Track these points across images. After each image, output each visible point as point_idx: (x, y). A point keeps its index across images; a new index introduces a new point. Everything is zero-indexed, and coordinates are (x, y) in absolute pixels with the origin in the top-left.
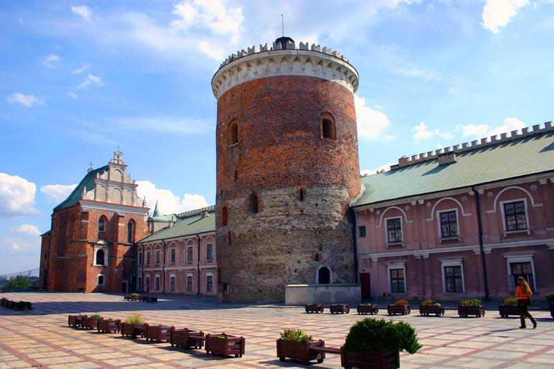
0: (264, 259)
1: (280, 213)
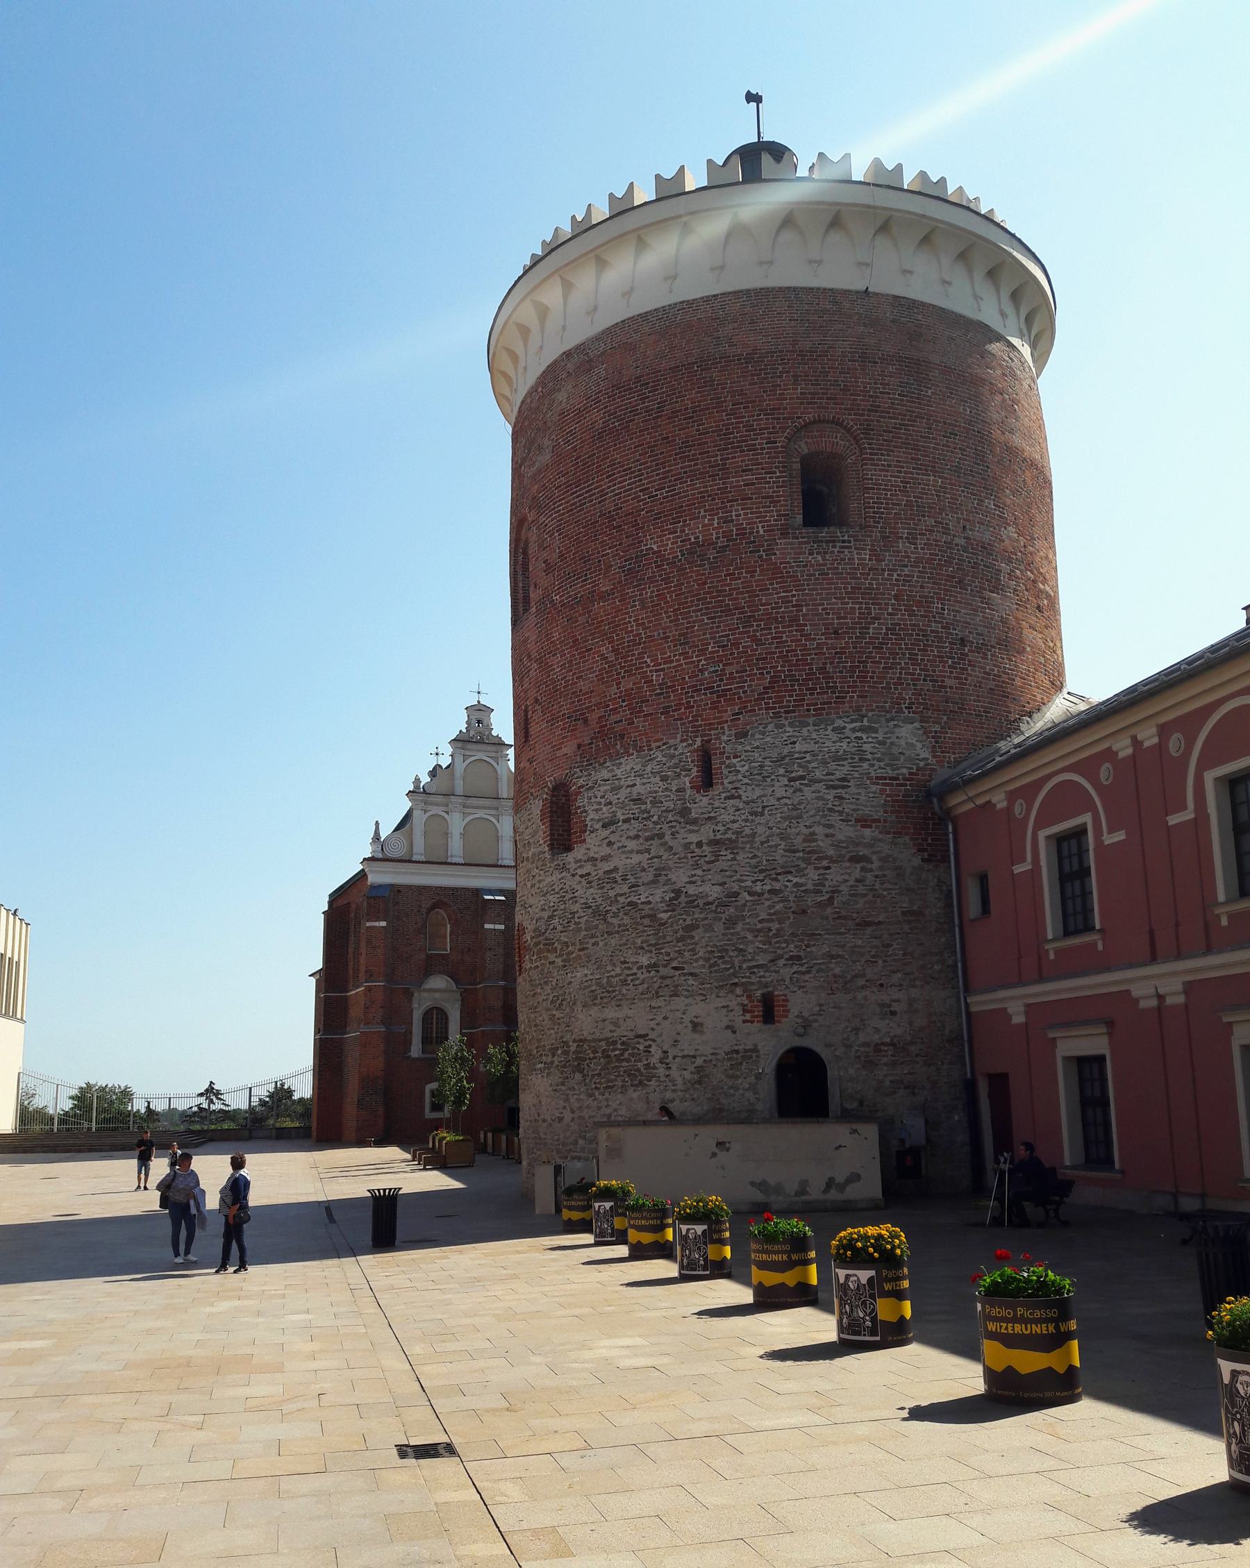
0: (586, 1022)
1: (632, 845)
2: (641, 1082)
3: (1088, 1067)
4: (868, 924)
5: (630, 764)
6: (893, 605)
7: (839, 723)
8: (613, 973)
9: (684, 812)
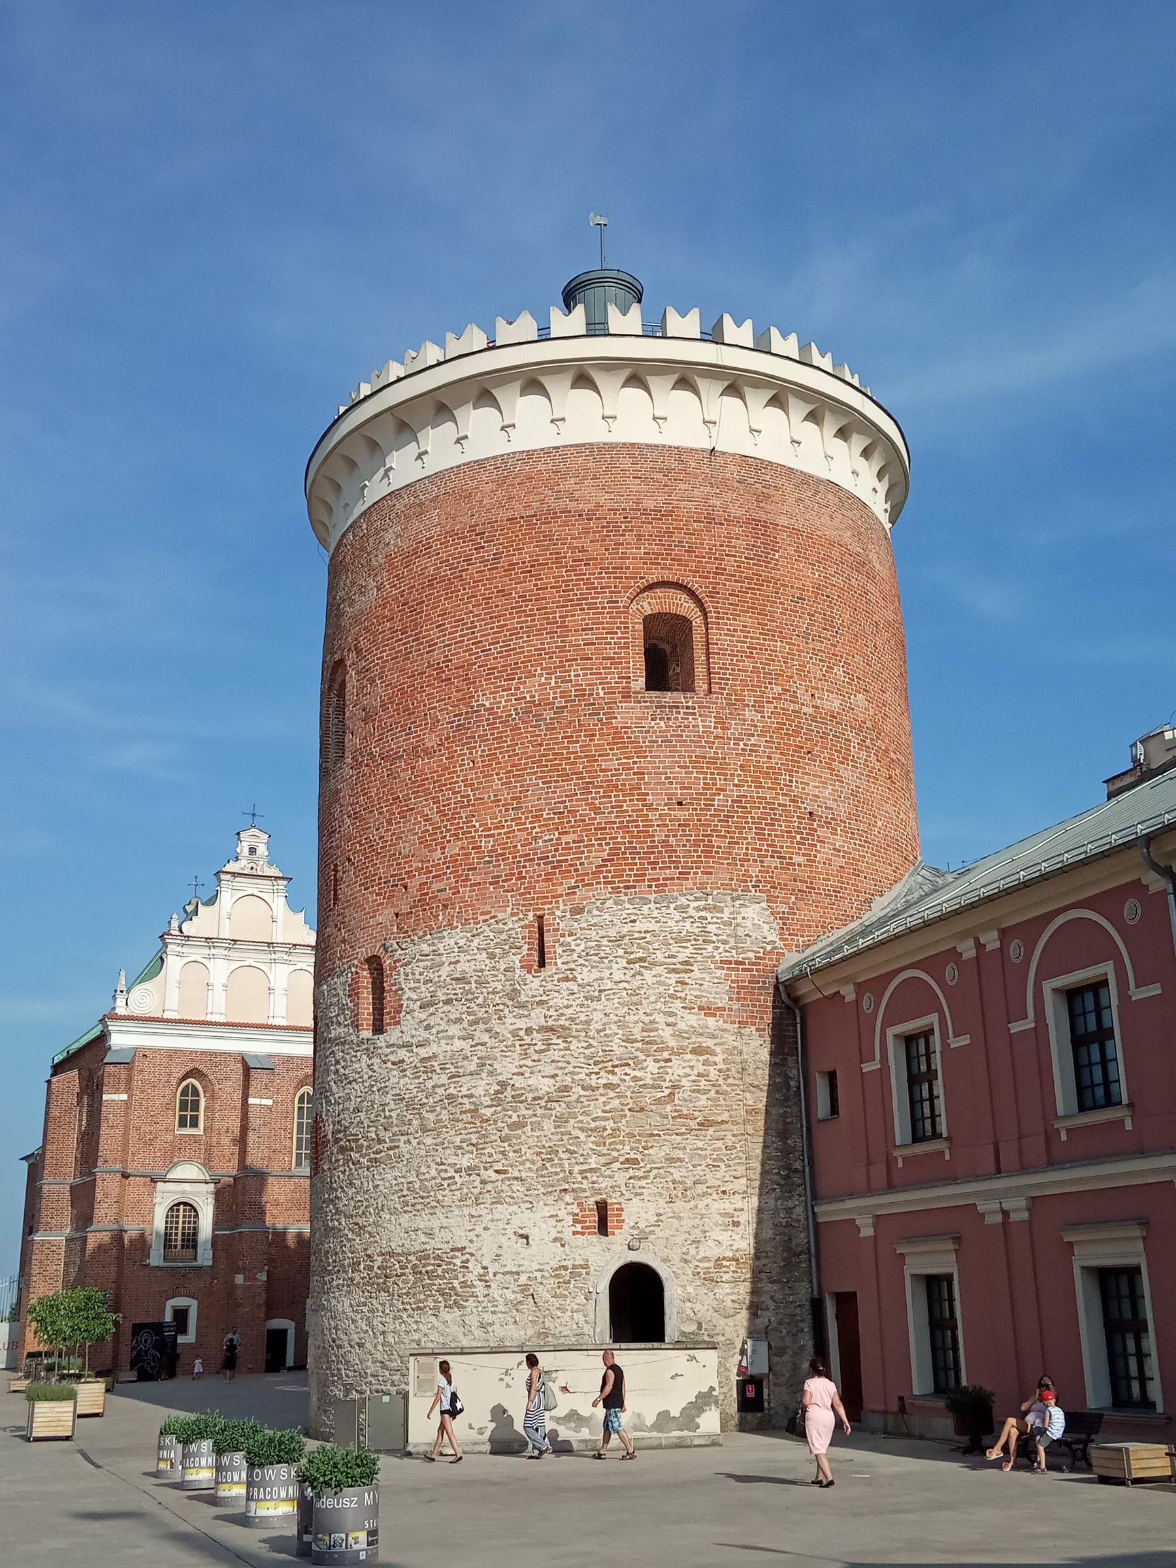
1: (454, 1030)
2: (455, 1302)
3: (935, 1287)
4: (711, 1123)
5: (452, 939)
6: (739, 775)
7: (683, 901)
8: (427, 1176)
9: (513, 994)
